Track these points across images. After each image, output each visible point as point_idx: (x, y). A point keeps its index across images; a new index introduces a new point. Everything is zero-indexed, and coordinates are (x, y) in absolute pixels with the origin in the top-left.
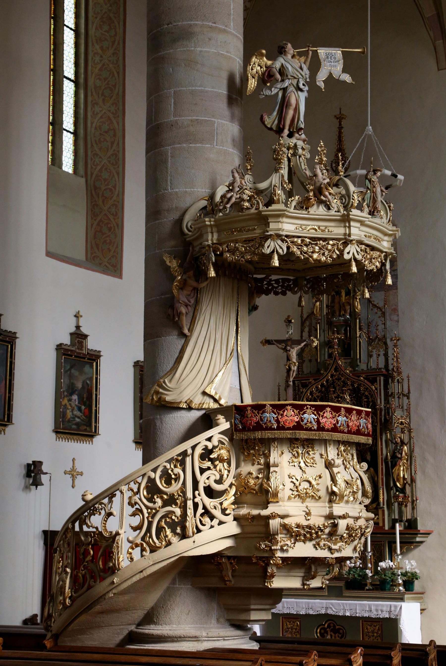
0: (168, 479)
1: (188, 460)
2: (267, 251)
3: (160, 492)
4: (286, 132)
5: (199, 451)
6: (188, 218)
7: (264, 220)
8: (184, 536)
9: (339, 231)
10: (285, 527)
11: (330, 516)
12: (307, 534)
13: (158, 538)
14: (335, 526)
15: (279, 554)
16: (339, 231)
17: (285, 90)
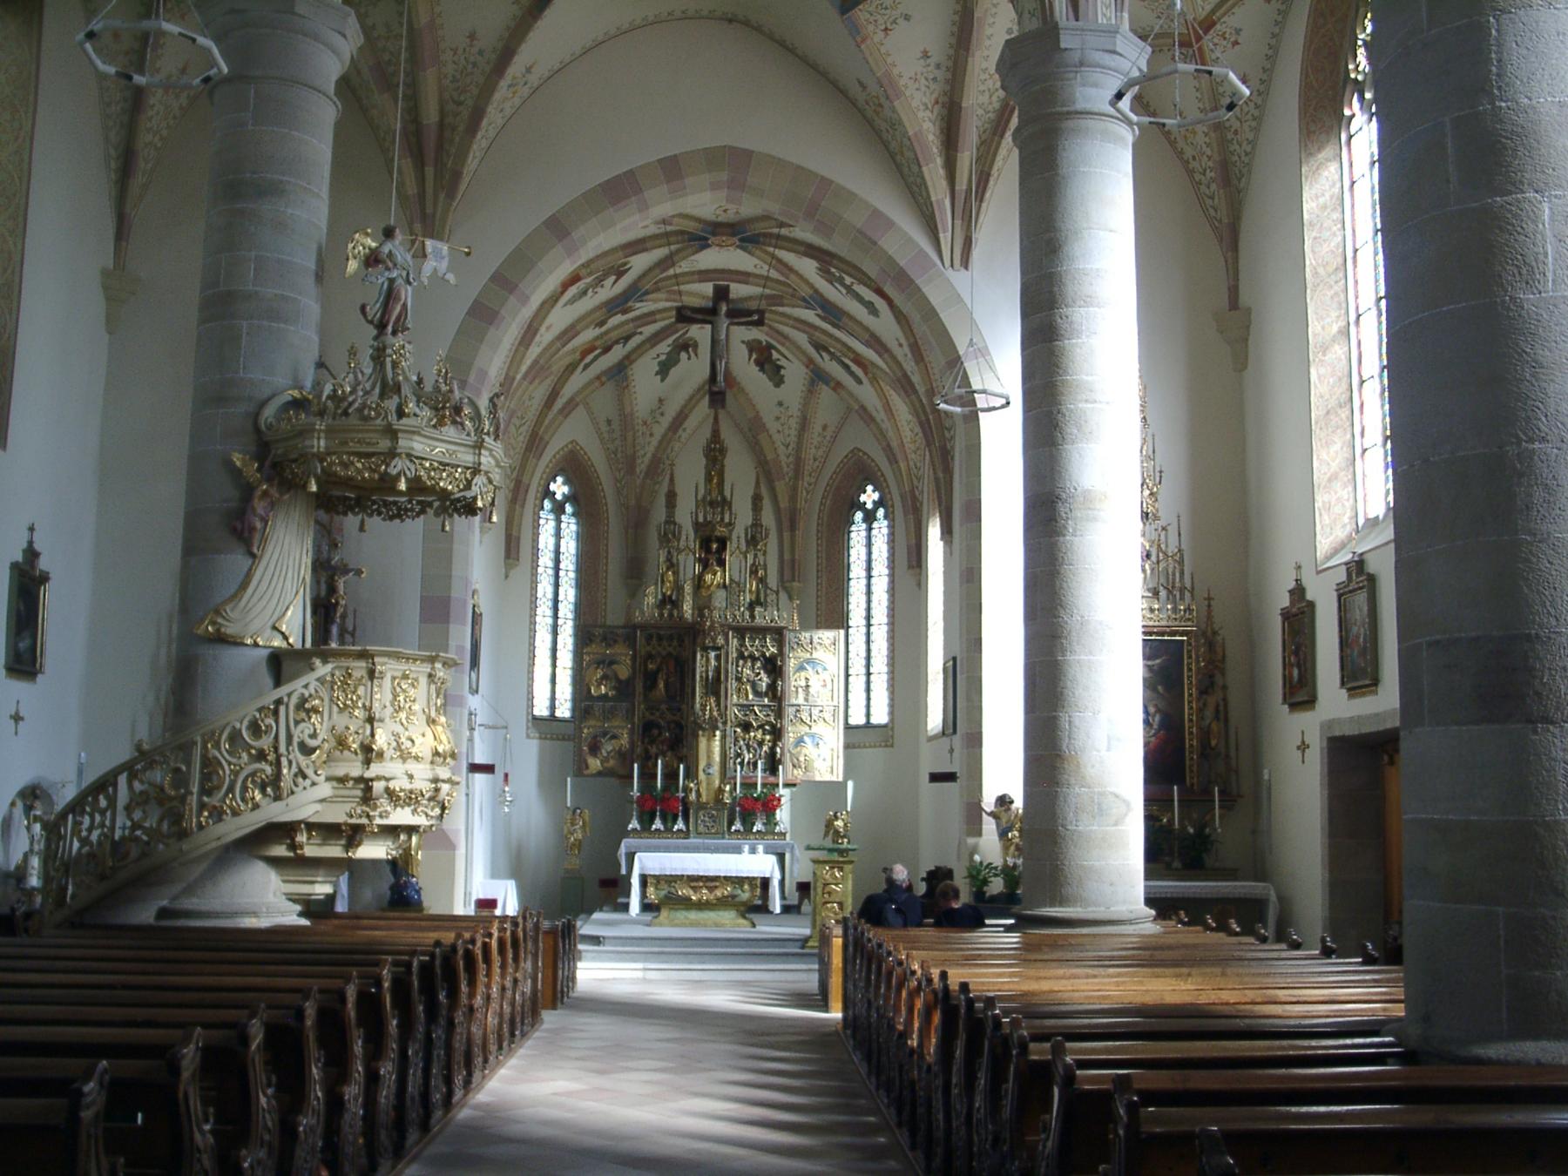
0: (255, 729)
1: (282, 709)
2: (394, 472)
3: (248, 747)
4: (390, 329)
5: (294, 700)
6: (269, 412)
7: (392, 433)
8: (277, 798)
9: (468, 458)
10: (387, 789)
11: (436, 780)
12: (411, 799)
13: (243, 799)
14: (437, 790)
15: (378, 821)
16: (468, 458)
17: (392, 281)
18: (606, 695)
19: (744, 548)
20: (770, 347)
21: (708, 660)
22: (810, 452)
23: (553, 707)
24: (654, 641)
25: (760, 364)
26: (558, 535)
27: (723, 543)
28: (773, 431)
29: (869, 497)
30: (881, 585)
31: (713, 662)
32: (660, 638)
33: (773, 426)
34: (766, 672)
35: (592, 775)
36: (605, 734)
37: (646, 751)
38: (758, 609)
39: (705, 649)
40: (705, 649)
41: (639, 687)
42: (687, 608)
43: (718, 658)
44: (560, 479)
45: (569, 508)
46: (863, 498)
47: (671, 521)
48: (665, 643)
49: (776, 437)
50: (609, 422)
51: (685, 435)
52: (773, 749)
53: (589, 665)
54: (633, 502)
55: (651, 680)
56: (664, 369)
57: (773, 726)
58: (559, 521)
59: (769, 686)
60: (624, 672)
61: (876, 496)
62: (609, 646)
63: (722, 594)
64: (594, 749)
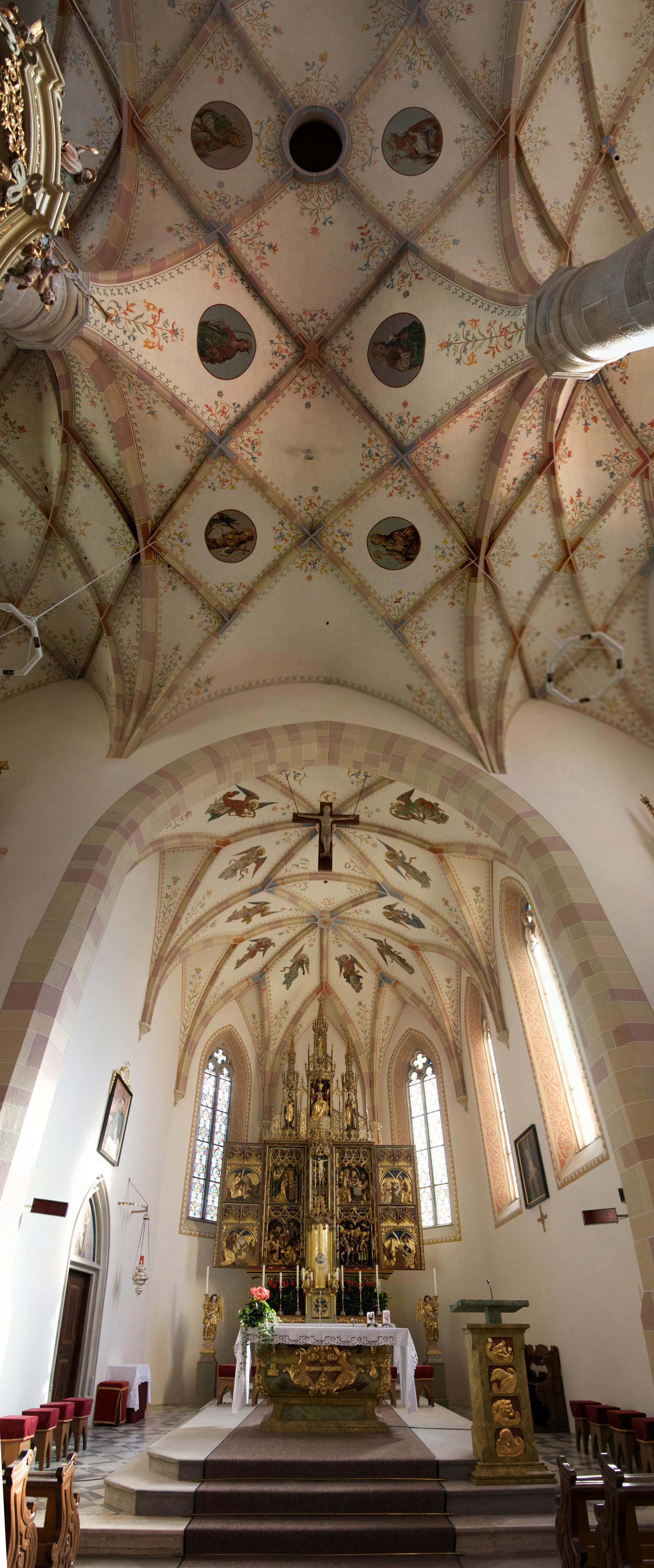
18: (241, 1198)
19: (341, 1087)
20: (354, 961)
21: (318, 1166)
22: (380, 1035)
23: (204, 1212)
24: (279, 1156)
25: (347, 977)
26: (217, 1086)
27: (327, 1085)
28: (356, 1023)
29: (420, 1061)
30: (435, 1120)
31: (321, 1167)
32: (283, 1153)
33: (355, 1019)
34: (361, 1180)
35: (227, 1266)
36: (239, 1231)
37: (271, 1244)
38: (353, 1132)
39: (315, 1157)
40: (315, 1157)
41: (267, 1191)
42: (303, 1129)
43: (325, 1165)
44: (221, 1051)
45: (225, 1071)
46: (416, 1063)
47: (292, 1072)
48: (286, 1157)
49: (358, 1027)
50: (254, 1016)
51: (301, 1030)
52: (369, 1243)
53: (230, 1174)
54: (268, 1069)
55: (276, 1187)
56: (289, 980)
57: (368, 1224)
58: (217, 1077)
59: (363, 1191)
60: (255, 1181)
61: (425, 1060)
62: (245, 1158)
63: (326, 1119)
64: (230, 1244)
